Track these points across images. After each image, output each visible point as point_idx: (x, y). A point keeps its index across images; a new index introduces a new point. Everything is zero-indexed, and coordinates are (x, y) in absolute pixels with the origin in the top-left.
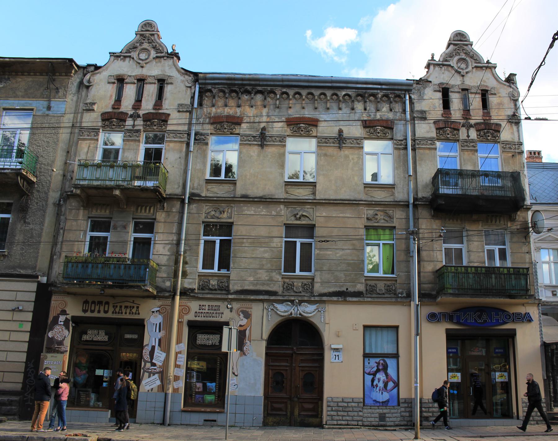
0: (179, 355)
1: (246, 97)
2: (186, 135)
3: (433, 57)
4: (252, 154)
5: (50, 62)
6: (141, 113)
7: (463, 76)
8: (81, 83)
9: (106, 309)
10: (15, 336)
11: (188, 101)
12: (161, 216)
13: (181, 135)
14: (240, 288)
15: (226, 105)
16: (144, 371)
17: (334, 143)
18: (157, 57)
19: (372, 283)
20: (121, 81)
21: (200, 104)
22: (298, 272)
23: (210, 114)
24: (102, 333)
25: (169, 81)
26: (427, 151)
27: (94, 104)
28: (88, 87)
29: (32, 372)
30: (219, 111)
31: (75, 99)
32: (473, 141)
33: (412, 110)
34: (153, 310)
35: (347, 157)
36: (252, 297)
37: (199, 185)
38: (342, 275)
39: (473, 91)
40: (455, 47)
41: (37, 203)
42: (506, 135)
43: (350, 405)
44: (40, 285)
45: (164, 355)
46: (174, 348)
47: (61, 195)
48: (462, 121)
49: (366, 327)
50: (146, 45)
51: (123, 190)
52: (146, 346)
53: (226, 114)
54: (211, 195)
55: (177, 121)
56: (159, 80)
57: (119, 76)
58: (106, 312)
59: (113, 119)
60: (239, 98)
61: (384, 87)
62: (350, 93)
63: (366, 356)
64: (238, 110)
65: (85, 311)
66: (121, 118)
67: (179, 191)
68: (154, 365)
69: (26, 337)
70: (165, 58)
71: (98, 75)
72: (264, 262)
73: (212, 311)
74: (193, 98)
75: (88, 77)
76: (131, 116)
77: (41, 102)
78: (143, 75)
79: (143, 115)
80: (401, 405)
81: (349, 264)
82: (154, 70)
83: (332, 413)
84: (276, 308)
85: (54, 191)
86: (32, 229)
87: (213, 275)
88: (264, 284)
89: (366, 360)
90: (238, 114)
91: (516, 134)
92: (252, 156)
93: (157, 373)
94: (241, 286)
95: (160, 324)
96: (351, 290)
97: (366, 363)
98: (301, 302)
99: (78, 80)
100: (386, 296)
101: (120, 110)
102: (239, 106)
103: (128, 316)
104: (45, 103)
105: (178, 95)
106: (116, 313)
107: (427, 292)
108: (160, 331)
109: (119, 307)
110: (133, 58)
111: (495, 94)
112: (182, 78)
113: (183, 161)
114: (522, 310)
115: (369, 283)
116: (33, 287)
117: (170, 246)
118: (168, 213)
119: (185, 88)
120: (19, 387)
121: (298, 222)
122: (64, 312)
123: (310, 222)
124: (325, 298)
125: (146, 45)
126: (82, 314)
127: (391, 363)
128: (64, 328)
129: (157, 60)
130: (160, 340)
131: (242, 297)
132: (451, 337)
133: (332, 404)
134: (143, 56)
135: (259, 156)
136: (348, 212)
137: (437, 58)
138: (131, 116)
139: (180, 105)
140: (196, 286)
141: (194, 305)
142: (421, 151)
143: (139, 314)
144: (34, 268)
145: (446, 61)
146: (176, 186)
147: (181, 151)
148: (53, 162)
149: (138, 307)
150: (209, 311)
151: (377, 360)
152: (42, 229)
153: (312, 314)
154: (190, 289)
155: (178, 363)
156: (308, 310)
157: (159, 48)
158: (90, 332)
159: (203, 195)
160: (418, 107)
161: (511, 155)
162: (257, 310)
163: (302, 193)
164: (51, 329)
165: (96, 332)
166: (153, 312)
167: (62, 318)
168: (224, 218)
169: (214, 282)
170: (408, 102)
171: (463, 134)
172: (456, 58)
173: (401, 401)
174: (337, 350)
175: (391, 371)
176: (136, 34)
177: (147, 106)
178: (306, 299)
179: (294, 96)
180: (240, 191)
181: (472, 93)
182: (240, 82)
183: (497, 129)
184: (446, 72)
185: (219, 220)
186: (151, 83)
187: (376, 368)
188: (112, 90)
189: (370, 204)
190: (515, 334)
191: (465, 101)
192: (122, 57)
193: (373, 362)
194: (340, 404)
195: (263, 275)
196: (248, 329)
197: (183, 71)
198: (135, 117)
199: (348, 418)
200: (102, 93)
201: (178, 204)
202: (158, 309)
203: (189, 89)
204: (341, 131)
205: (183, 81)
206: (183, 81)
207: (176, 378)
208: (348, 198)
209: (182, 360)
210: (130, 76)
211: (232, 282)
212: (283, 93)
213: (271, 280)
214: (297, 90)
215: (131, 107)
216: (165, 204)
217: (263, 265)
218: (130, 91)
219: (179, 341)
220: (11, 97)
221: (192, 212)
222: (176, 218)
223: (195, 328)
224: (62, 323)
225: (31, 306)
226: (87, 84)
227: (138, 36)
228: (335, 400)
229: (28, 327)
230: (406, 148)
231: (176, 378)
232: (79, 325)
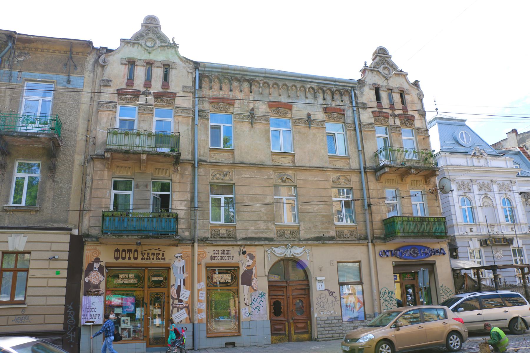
0: (200, 292)
1: (236, 84)
2: (191, 112)
3: (366, 65)
4: (245, 129)
5: (71, 42)
6: (152, 91)
7: (387, 79)
8: (96, 62)
9: (136, 256)
10: (52, 282)
11: (190, 84)
12: (176, 178)
13: (187, 111)
14: (244, 236)
15: (221, 89)
16: (173, 307)
17: (305, 124)
18: (162, 46)
19: (340, 229)
20: (132, 63)
21: (200, 87)
23: (209, 95)
24: (132, 276)
25: (173, 66)
26: (369, 133)
28: (103, 67)
29: (72, 313)
30: (215, 93)
31: (91, 75)
32: (398, 127)
33: (357, 103)
34: (176, 256)
35: (314, 135)
36: (256, 243)
37: (205, 153)
40: (381, 58)
41: (64, 164)
42: (418, 123)
43: (333, 322)
44: (72, 236)
46: (197, 286)
47: (85, 157)
48: (390, 112)
51: (149, 154)
52: (173, 286)
54: (214, 161)
56: (147, 64)
57: (130, 58)
58: (136, 259)
59: (127, 94)
60: (231, 84)
61: (338, 83)
62: (313, 86)
65: (117, 258)
66: (136, 94)
67: (189, 157)
68: (181, 301)
69: (64, 283)
70: (169, 47)
71: (112, 56)
72: (261, 215)
73: (224, 255)
74: (194, 81)
75: (102, 57)
76: (144, 93)
77: (61, 76)
78: (151, 60)
79: (154, 93)
80: (368, 319)
81: (323, 216)
82: (159, 56)
83: (321, 329)
84: (274, 251)
85: (78, 154)
86: (61, 187)
87: (222, 226)
89: (341, 287)
90: (231, 97)
92: (244, 131)
93: (184, 307)
94: (245, 235)
95: (183, 267)
96: (327, 235)
99: (93, 60)
100: (350, 239)
101: (133, 88)
102: (231, 91)
103: (155, 261)
104: (65, 78)
106: (144, 259)
107: (378, 236)
108: (183, 273)
109: (146, 254)
110: (141, 45)
111: (409, 94)
112: (183, 65)
113: (190, 132)
115: (338, 229)
116: (67, 238)
117: (186, 202)
118: (182, 175)
119: (186, 73)
120: (60, 327)
122: (97, 260)
125: (151, 35)
126: (115, 261)
128: (99, 274)
129: (162, 48)
130: (184, 280)
132: (396, 267)
134: (149, 44)
135: (250, 131)
136: (319, 177)
137: (368, 65)
138: (144, 93)
140: (209, 235)
141: (209, 251)
143: (164, 259)
144: (66, 222)
145: (376, 68)
146: (187, 153)
147: (188, 125)
148: (76, 128)
149: (163, 254)
150: (222, 255)
152: (70, 188)
153: (300, 255)
154: (205, 238)
155: (200, 298)
156: (297, 251)
157: (162, 39)
158: (120, 276)
159: (208, 161)
160: (361, 100)
161: (422, 138)
162: (259, 252)
163: (286, 161)
164: (87, 275)
165: (126, 275)
166: (177, 257)
167: (96, 265)
168: (227, 180)
169: (223, 231)
170: (353, 96)
171: (391, 121)
172: (383, 66)
173: (368, 316)
174: (320, 281)
176: (142, 26)
177: (157, 86)
178: (296, 243)
179: (272, 86)
180: (238, 159)
181: (394, 92)
182: (233, 72)
183: (412, 118)
184: (376, 76)
185: (223, 182)
186: (158, 67)
188: (124, 70)
190: (435, 263)
191: (390, 97)
192: (131, 44)
194: (326, 322)
196: (254, 268)
197: (184, 59)
199: (332, 332)
200: (117, 71)
201: (189, 169)
202: (181, 255)
203: (190, 74)
204: (309, 116)
205: (184, 68)
206: (184, 68)
207: (200, 311)
208: (318, 165)
209: (202, 295)
210: (140, 60)
211: (238, 232)
212: (264, 83)
213: (268, 229)
214: (274, 81)
215: (142, 86)
216: (179, 168)
217: (261, 217)
218: (140, 73)
220: (32, 70)
221: (201, 174)
222: (189, 179)
223: (211, 270)
224: (97, 269)
225: (66, 256)
226: (103, 64)
227: (144, 27)
228: (322, 319)
229: (65, 273)
230: (355, 130)
231: (200, 311)
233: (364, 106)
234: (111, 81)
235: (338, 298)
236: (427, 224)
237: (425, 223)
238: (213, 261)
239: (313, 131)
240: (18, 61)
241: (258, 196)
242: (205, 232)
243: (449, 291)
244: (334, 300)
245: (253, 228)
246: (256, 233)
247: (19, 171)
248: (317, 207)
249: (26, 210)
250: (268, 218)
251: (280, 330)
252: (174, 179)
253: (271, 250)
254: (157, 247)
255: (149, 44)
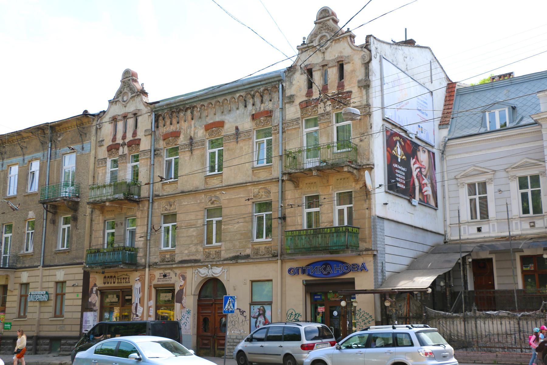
0: (151, 309)
6: (127, 141)
14: (180, 259)
18: (133, 97)
22: (214, 243)
26: (294, 131)
27: (103, 140)
32: (328, 114)
38: (237, 243)
39: (330, 65)
45: (142, 308)
49: (252, 281)
50: (125, 90)
53: (171, 131)
55: (145, 144)
58: (114, 283)
61: (262, 83)
62: (242, 94)
63: (252, 303)
64: (178, 126)
65: (105, 283)
68: (137, 316)
72: (193, 239)
76: (122, 145)
81: (242, 234)
88: (193, 255)
89: (252, 306)
91: (365, 97)
96: (243, 254)
97: (252, 310)
98: (212, 265)
104: (81, 146)
105: (146, 122)
114: (359, 261)
115: (256, 247)
121: (213, 206)
122: (95, 285)
123: (219, 205)
124: (225, 262)
127: (267, 308)
131: (180, 265)
133: (230, 340)
138: (122, 145)
139: (146, 131)
141: (157, 274)
142: (289, 132)
151: (259, 307)
152: (85, 232)
156: (217, 272)
158: (109, 296)
160: (288, 93)
162: (189, 273)
167: (95, 289)
168: (172, 210)
170: (280, 90)
175: (268, 314)
182: (175, 105)
187: (258, 313)
189: (258, 183)
191: (325, 76)
193: (256, 308)
195: (193, 249)
198: (123, 145)
201: (147, 203)
204: (237, 128)
210: (119, 115)
213: (197, 251)
214: (209, 101)
215: (121, 138)
219: (150, 299)
223: (159, 290)
229: (80, 296)
232: (103, 293)
233: (291, 99)
234: (103, 140)
235: (248, 318)
236: (322, 237)
237: (320, 236)
238: (159, 283)
239: (241, 144)
240: (59, 141)
241: (192, 221)
242: (155, 258)
243: (368, 317)
244: (244, 320)
245: (186, 252)
246: (189, 256)
247: (66, 223)
248: (237, 226)
249: (64, 252)
250: (198, 241)
251: (206, 344)
252: (137, 215)
253: (196, 271)
254: (125, 273)
255: (125, 99)
